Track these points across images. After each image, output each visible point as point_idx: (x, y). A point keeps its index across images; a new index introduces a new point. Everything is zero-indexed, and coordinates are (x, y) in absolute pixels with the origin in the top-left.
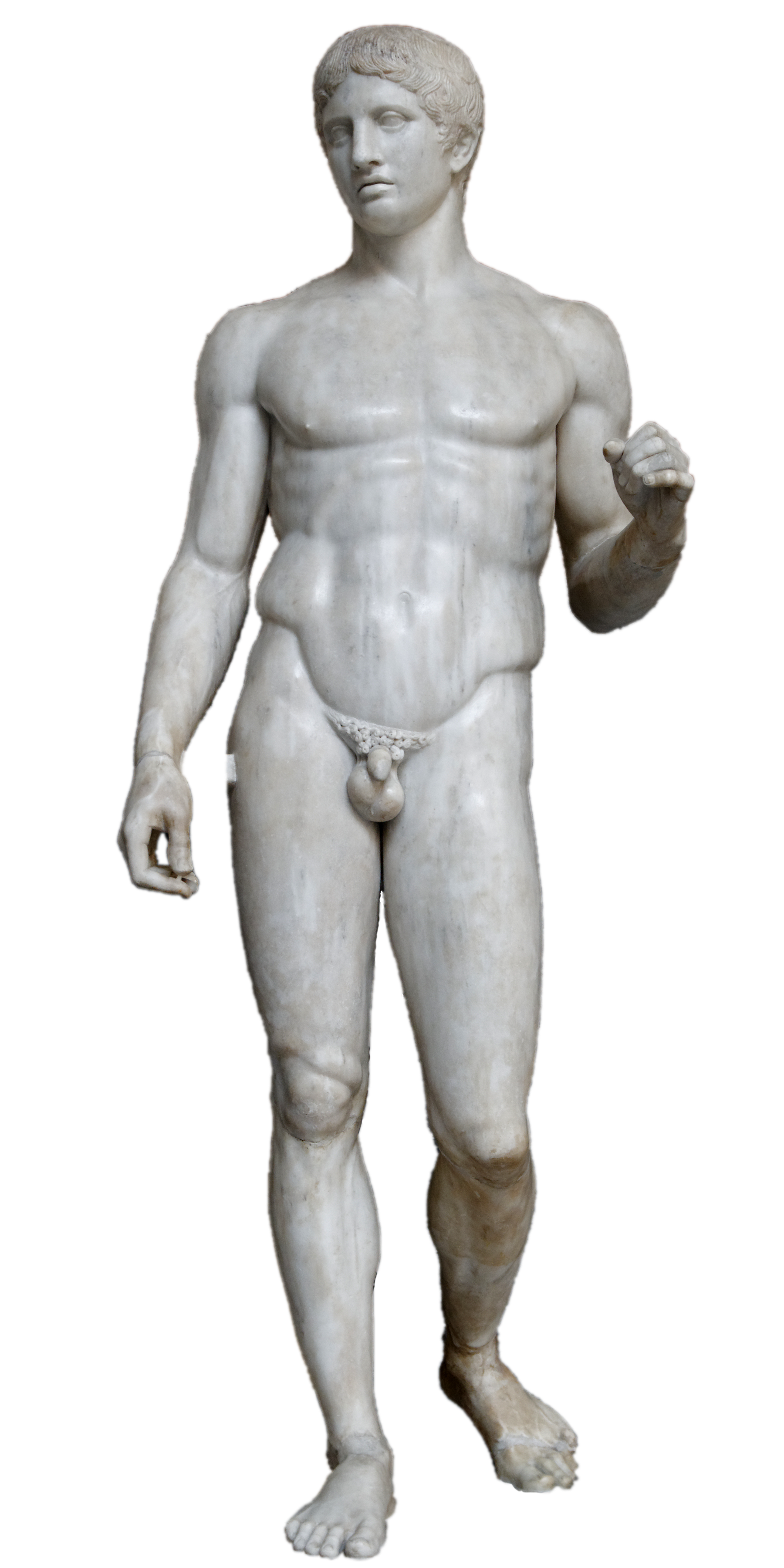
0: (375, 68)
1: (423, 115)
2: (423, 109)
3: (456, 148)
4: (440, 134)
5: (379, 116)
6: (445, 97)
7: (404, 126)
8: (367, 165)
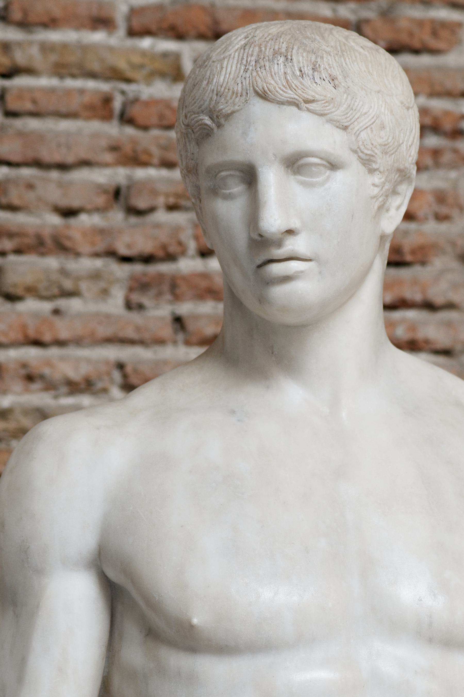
0: (291, 94)
1: (353, 160)
2: (355, 152)
3: (390, 200)
4: (374, 185)
5: (294, 163)
6: (382, 133)
7: (328, 178)
8: (280, 236)
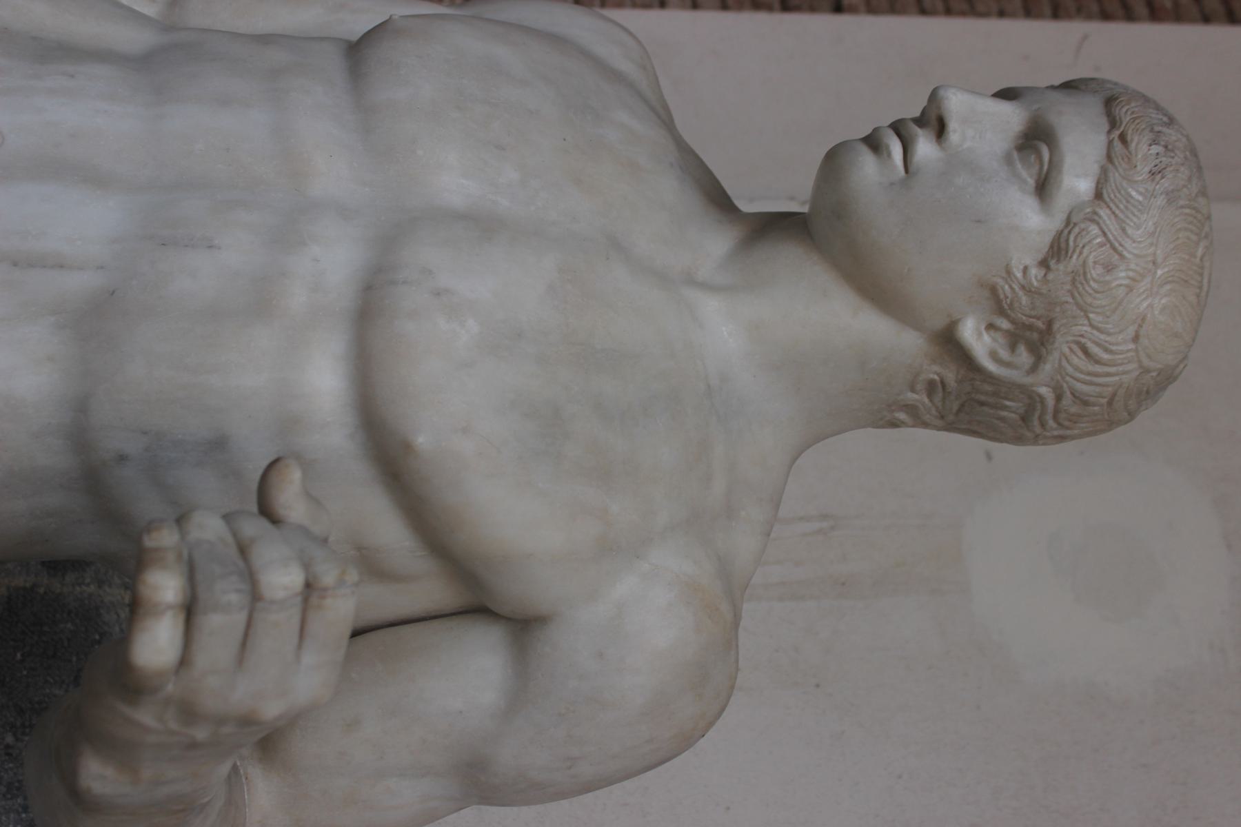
1: (1056, 223)
2: (1068, 222)
3: (1005, 324)
4: (1025, 270)
